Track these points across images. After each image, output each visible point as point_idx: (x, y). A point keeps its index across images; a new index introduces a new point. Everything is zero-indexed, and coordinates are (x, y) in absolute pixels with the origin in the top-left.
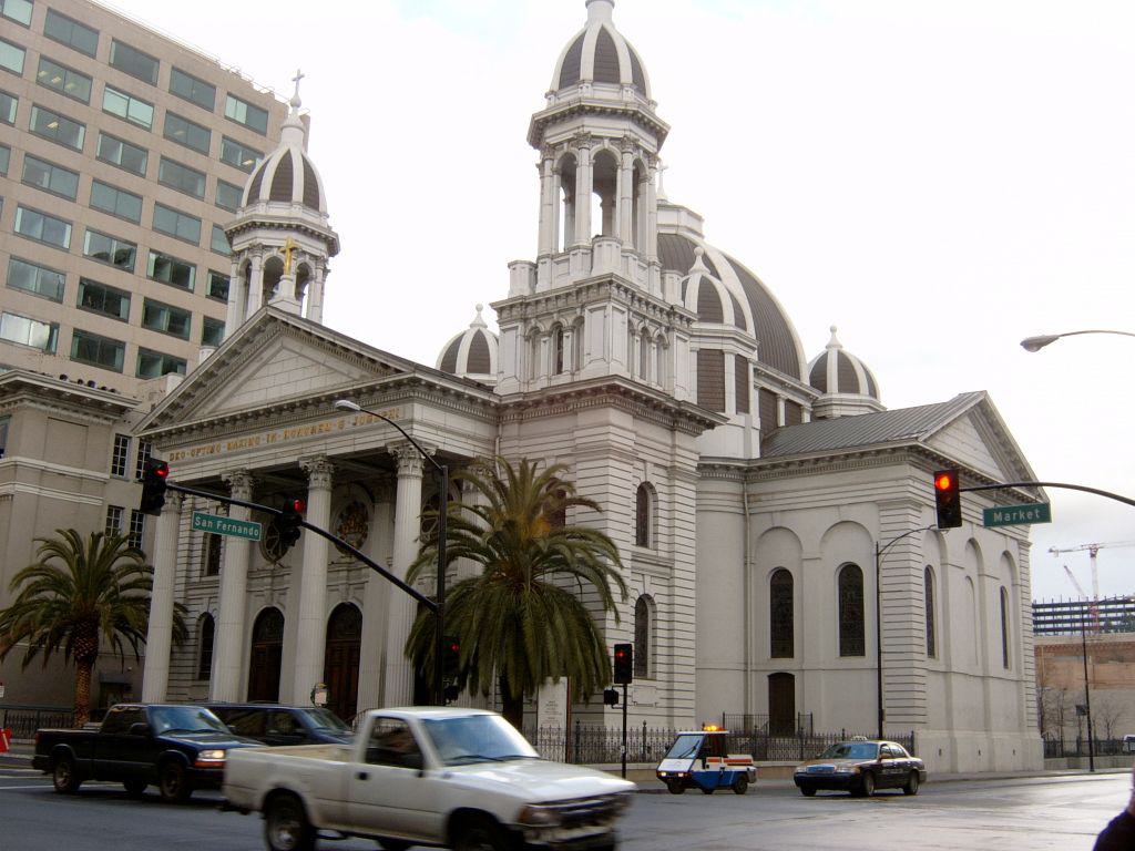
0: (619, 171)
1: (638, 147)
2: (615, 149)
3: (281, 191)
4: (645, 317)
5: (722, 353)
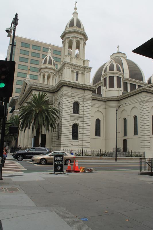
2: (72, 39)
3: (45, 63)
4: (77, 69)
5: (113, 77)
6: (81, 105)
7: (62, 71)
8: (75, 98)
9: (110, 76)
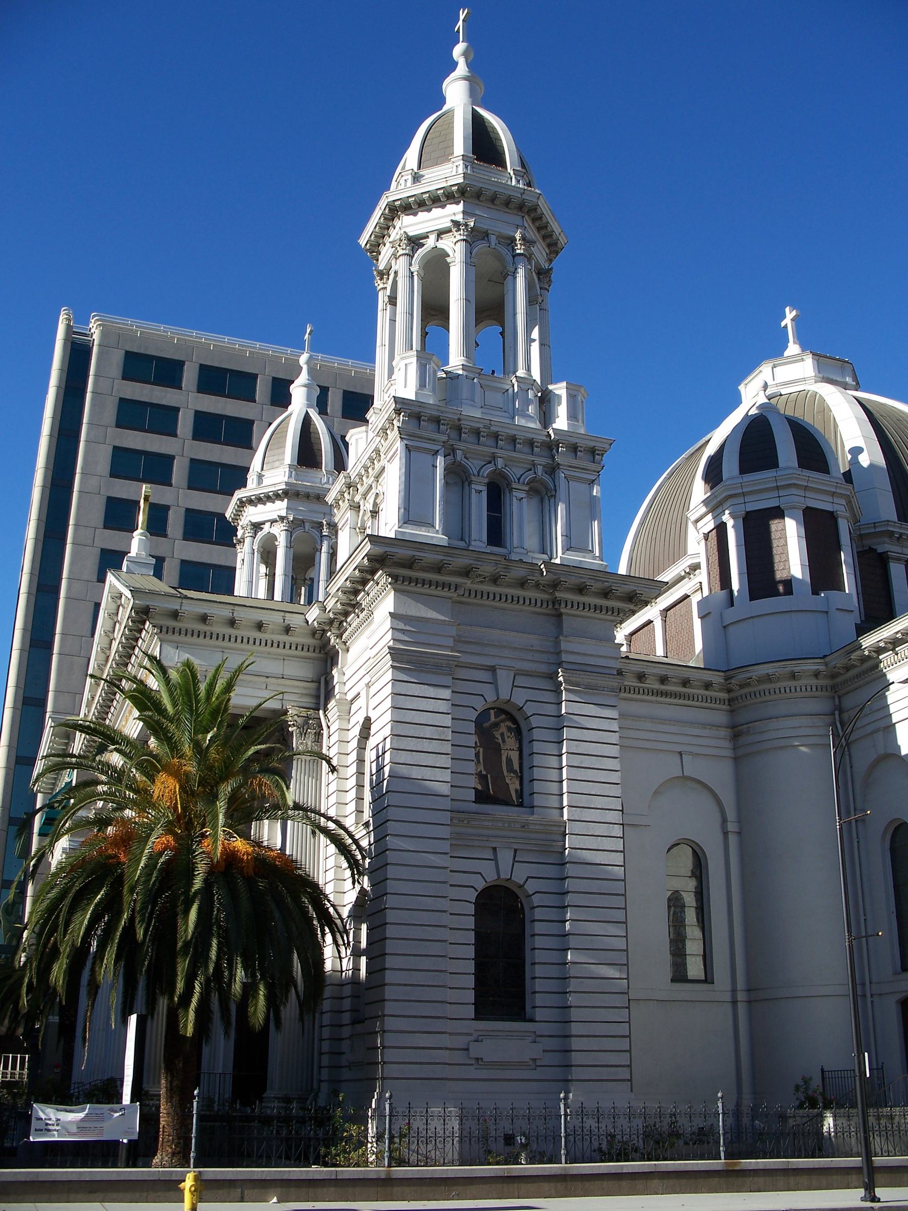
6: (536, 734)
7: (377, 477)
8: (485, 676)
9: (751, 507)
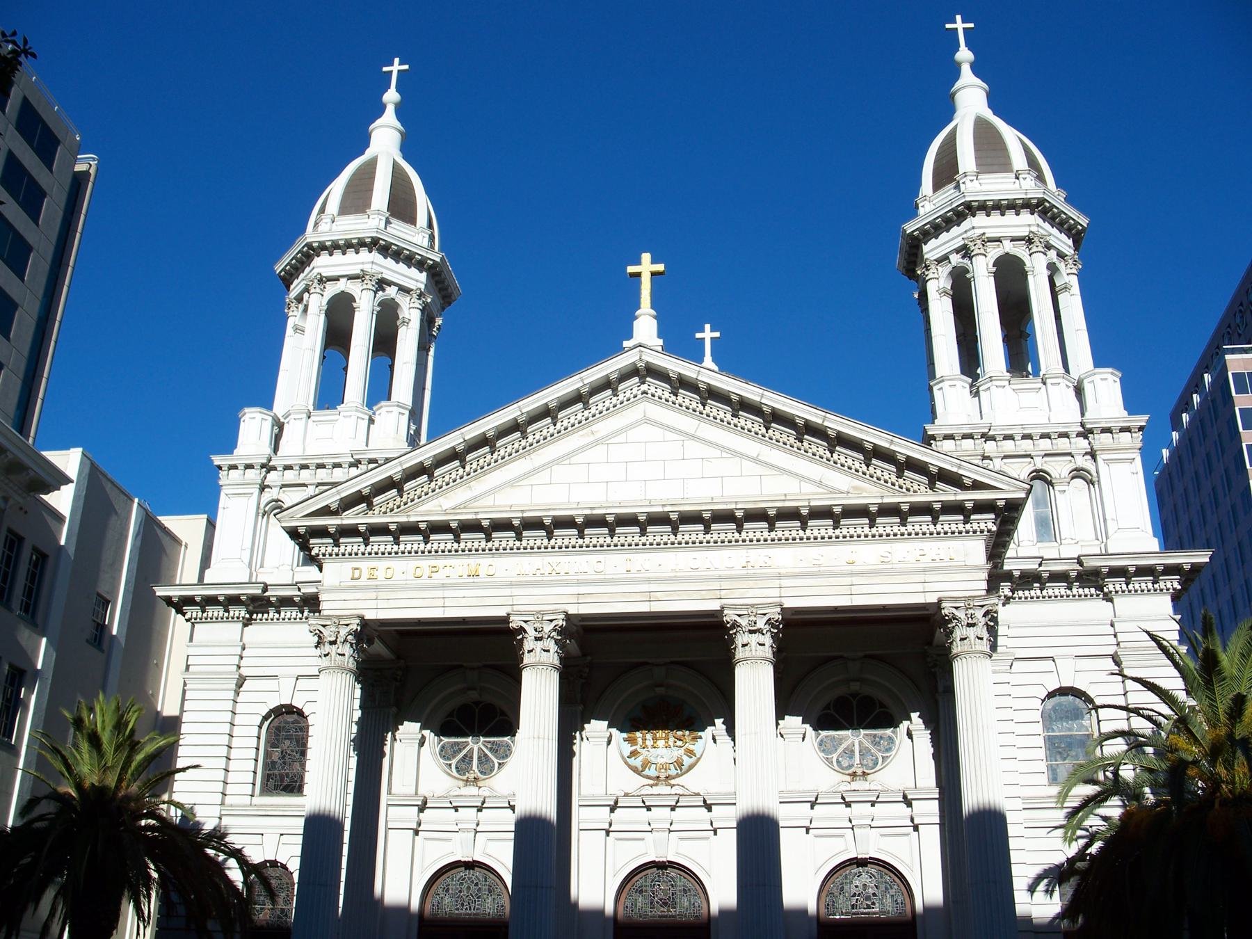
0: (1030, 278)
1: (1048, 247)
2: (1020, 251)
